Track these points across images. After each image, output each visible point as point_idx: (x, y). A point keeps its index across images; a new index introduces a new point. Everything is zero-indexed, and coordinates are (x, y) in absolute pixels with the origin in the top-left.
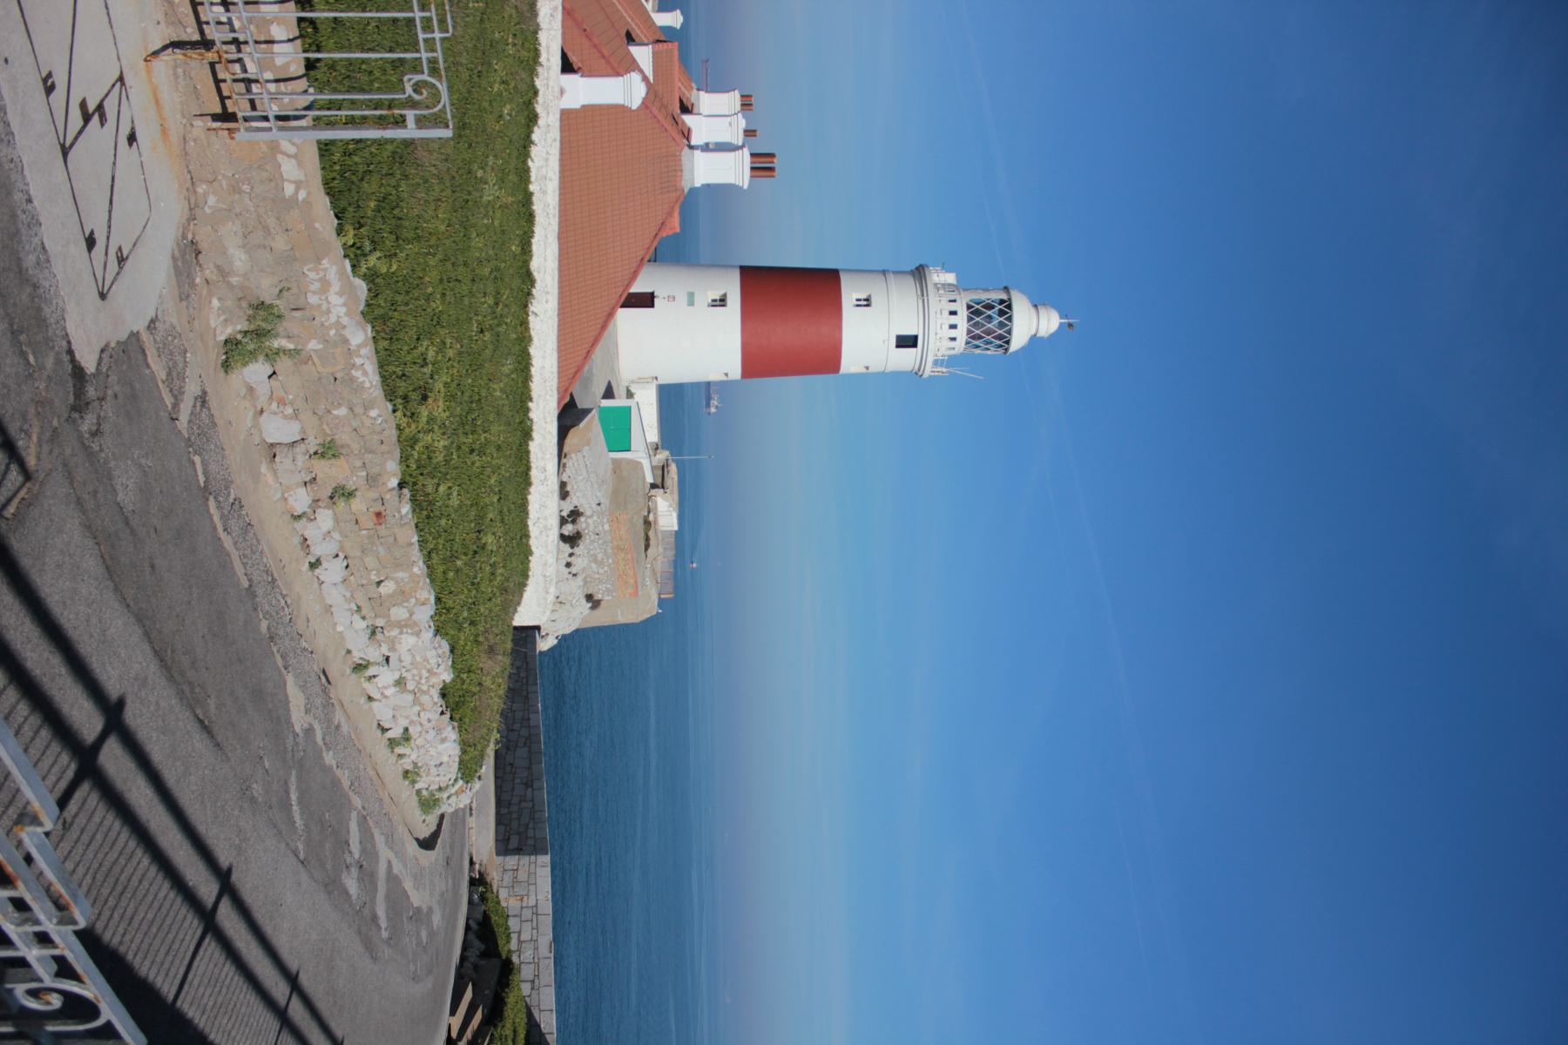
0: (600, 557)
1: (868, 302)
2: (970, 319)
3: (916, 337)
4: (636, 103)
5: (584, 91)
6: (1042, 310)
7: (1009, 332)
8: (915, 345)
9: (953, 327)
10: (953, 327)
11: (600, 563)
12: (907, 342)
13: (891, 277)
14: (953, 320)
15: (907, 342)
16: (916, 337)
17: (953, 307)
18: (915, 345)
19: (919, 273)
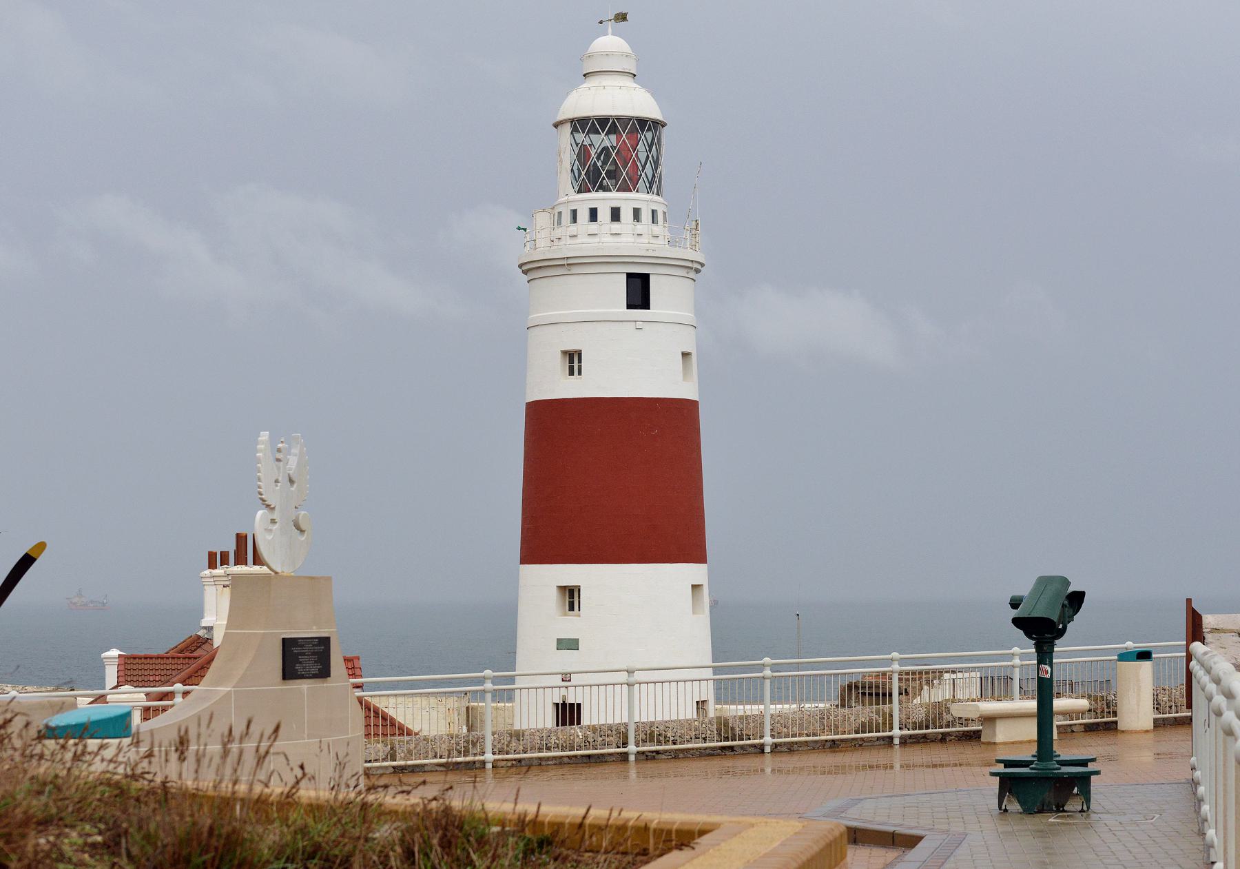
1: (573, 359)
2: (604, 188)
3: (630, 276)
8: (645, 278)
10: (616, 215)
12: (639, 292)
14: (604, 215)
15: (639, 292)
16: (630, 276)
17: (583, 215)
18: (645, 278)
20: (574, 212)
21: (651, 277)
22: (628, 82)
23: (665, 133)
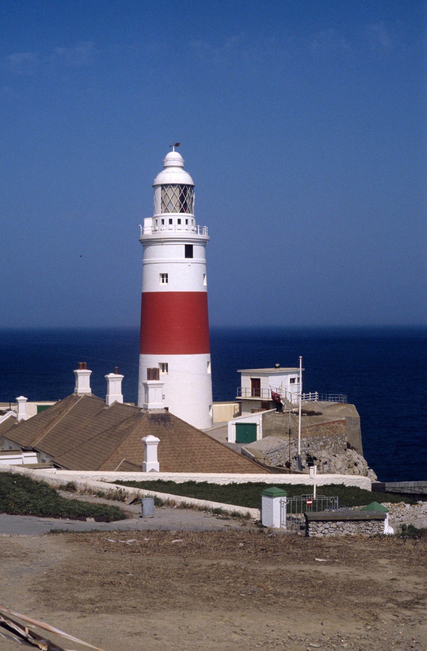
0: (321, 443)
1: (165, 276)
3: (186, 246)
4: (157, 439)
5: (152, 461)
6: (167, 164)
7: (182, 186)
9: (179, 221)
11: (326, 444)
13: (146, 260)
14: (175, 222)
15: (189, 252)
16: (186, 246)
17: (167, 222)
19: (147, 243)
20: (163, 221)
21: (194, 246)
22: (180, 170)
23: (194, 188)
